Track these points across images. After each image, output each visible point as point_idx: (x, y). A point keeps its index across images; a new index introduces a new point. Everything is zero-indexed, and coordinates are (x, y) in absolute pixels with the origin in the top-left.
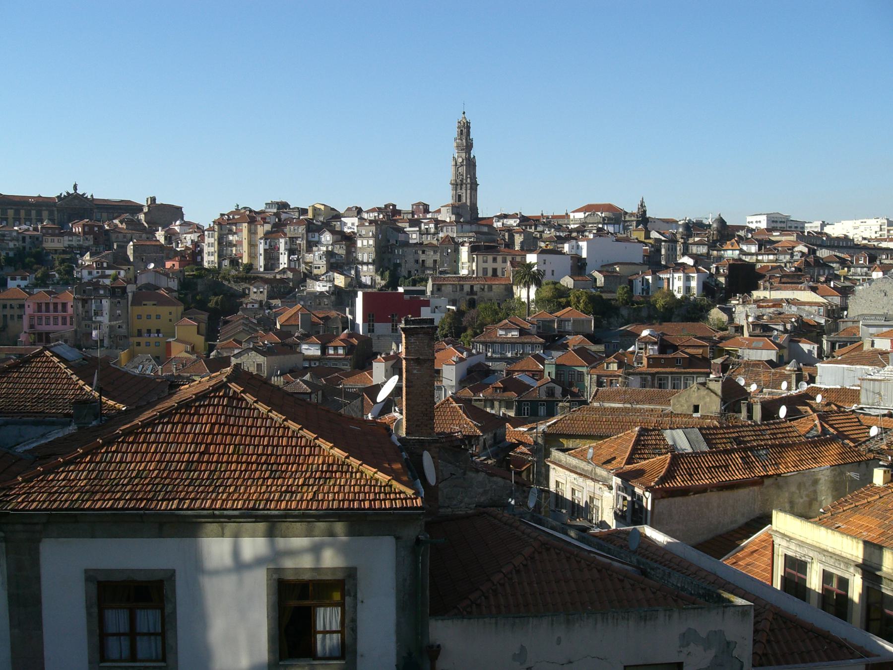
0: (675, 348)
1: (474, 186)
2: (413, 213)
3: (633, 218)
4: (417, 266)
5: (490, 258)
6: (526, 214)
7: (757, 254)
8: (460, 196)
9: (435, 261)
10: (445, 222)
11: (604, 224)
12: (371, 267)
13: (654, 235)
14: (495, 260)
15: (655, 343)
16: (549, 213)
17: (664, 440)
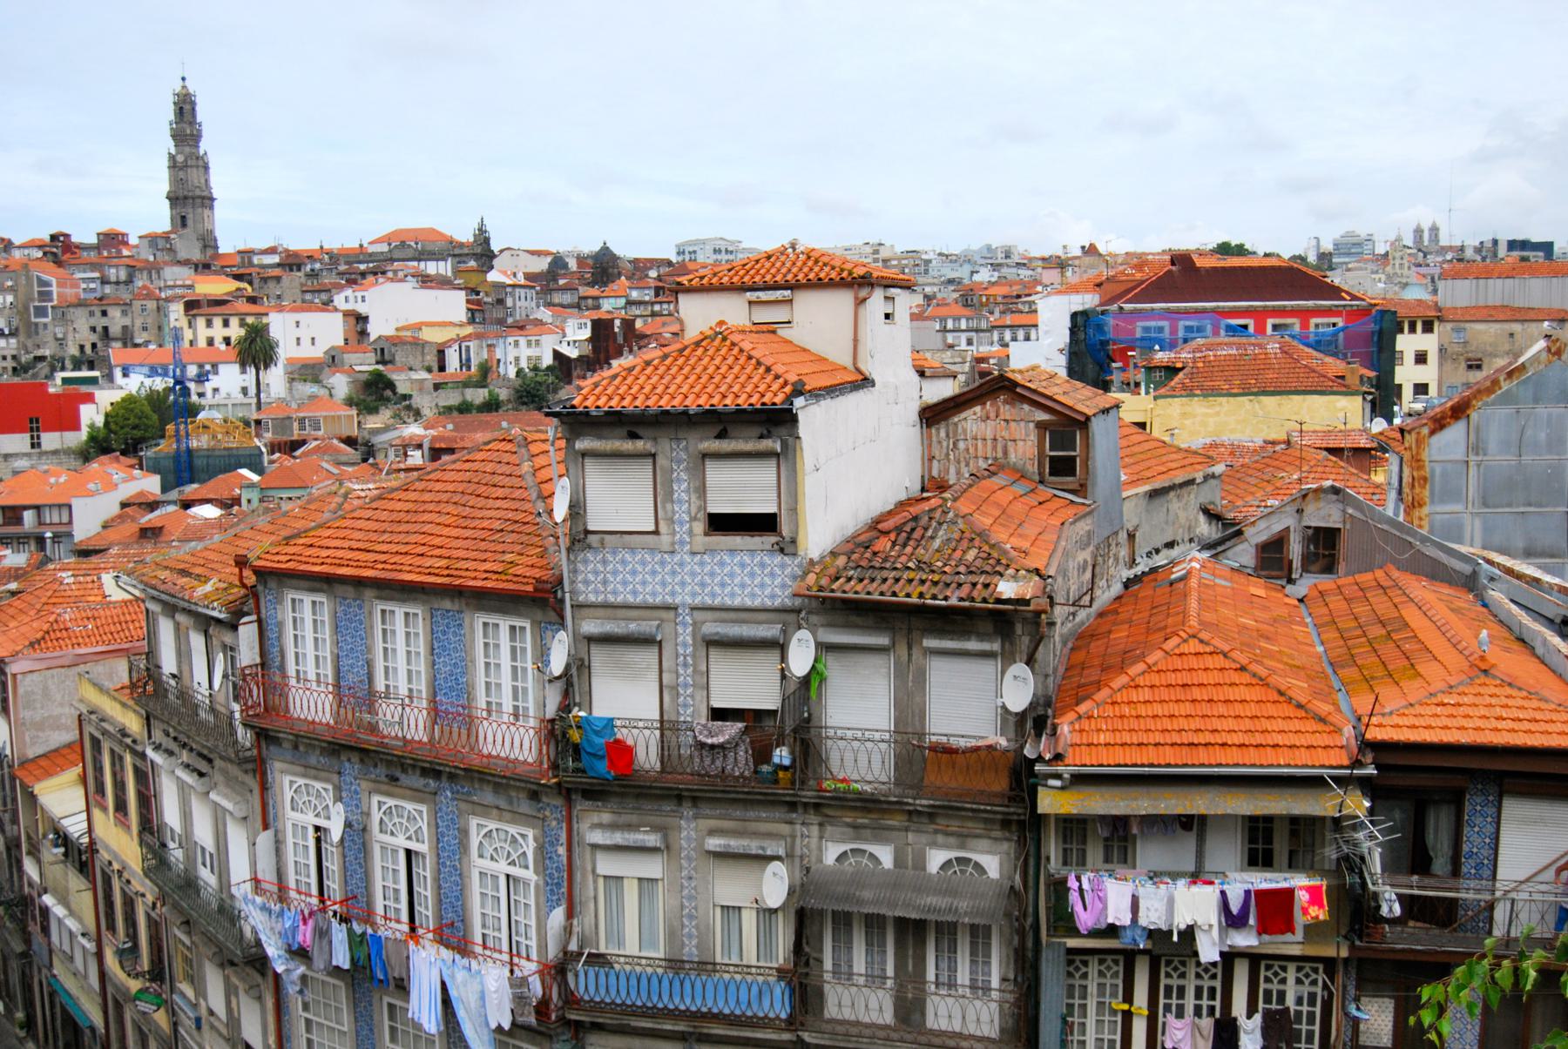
0: (451, 451)
1: (208, 201)
2: (97, 248)
3: (466, 251)
4: (94, 338)
5: (218, 322)
6: (294, 246)
7: (653, 304)
8: (183, 218)
9: (125, 328)
10: (147, 261)
11: (420, 260)
12: (13, 341)
13: (493, 276)
14: (226, 324)
15: (420, 446)
16: (333, 244)
17: (101, 587)
